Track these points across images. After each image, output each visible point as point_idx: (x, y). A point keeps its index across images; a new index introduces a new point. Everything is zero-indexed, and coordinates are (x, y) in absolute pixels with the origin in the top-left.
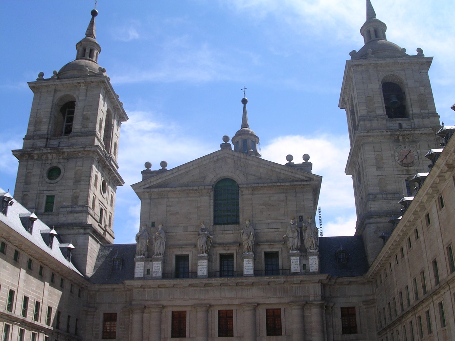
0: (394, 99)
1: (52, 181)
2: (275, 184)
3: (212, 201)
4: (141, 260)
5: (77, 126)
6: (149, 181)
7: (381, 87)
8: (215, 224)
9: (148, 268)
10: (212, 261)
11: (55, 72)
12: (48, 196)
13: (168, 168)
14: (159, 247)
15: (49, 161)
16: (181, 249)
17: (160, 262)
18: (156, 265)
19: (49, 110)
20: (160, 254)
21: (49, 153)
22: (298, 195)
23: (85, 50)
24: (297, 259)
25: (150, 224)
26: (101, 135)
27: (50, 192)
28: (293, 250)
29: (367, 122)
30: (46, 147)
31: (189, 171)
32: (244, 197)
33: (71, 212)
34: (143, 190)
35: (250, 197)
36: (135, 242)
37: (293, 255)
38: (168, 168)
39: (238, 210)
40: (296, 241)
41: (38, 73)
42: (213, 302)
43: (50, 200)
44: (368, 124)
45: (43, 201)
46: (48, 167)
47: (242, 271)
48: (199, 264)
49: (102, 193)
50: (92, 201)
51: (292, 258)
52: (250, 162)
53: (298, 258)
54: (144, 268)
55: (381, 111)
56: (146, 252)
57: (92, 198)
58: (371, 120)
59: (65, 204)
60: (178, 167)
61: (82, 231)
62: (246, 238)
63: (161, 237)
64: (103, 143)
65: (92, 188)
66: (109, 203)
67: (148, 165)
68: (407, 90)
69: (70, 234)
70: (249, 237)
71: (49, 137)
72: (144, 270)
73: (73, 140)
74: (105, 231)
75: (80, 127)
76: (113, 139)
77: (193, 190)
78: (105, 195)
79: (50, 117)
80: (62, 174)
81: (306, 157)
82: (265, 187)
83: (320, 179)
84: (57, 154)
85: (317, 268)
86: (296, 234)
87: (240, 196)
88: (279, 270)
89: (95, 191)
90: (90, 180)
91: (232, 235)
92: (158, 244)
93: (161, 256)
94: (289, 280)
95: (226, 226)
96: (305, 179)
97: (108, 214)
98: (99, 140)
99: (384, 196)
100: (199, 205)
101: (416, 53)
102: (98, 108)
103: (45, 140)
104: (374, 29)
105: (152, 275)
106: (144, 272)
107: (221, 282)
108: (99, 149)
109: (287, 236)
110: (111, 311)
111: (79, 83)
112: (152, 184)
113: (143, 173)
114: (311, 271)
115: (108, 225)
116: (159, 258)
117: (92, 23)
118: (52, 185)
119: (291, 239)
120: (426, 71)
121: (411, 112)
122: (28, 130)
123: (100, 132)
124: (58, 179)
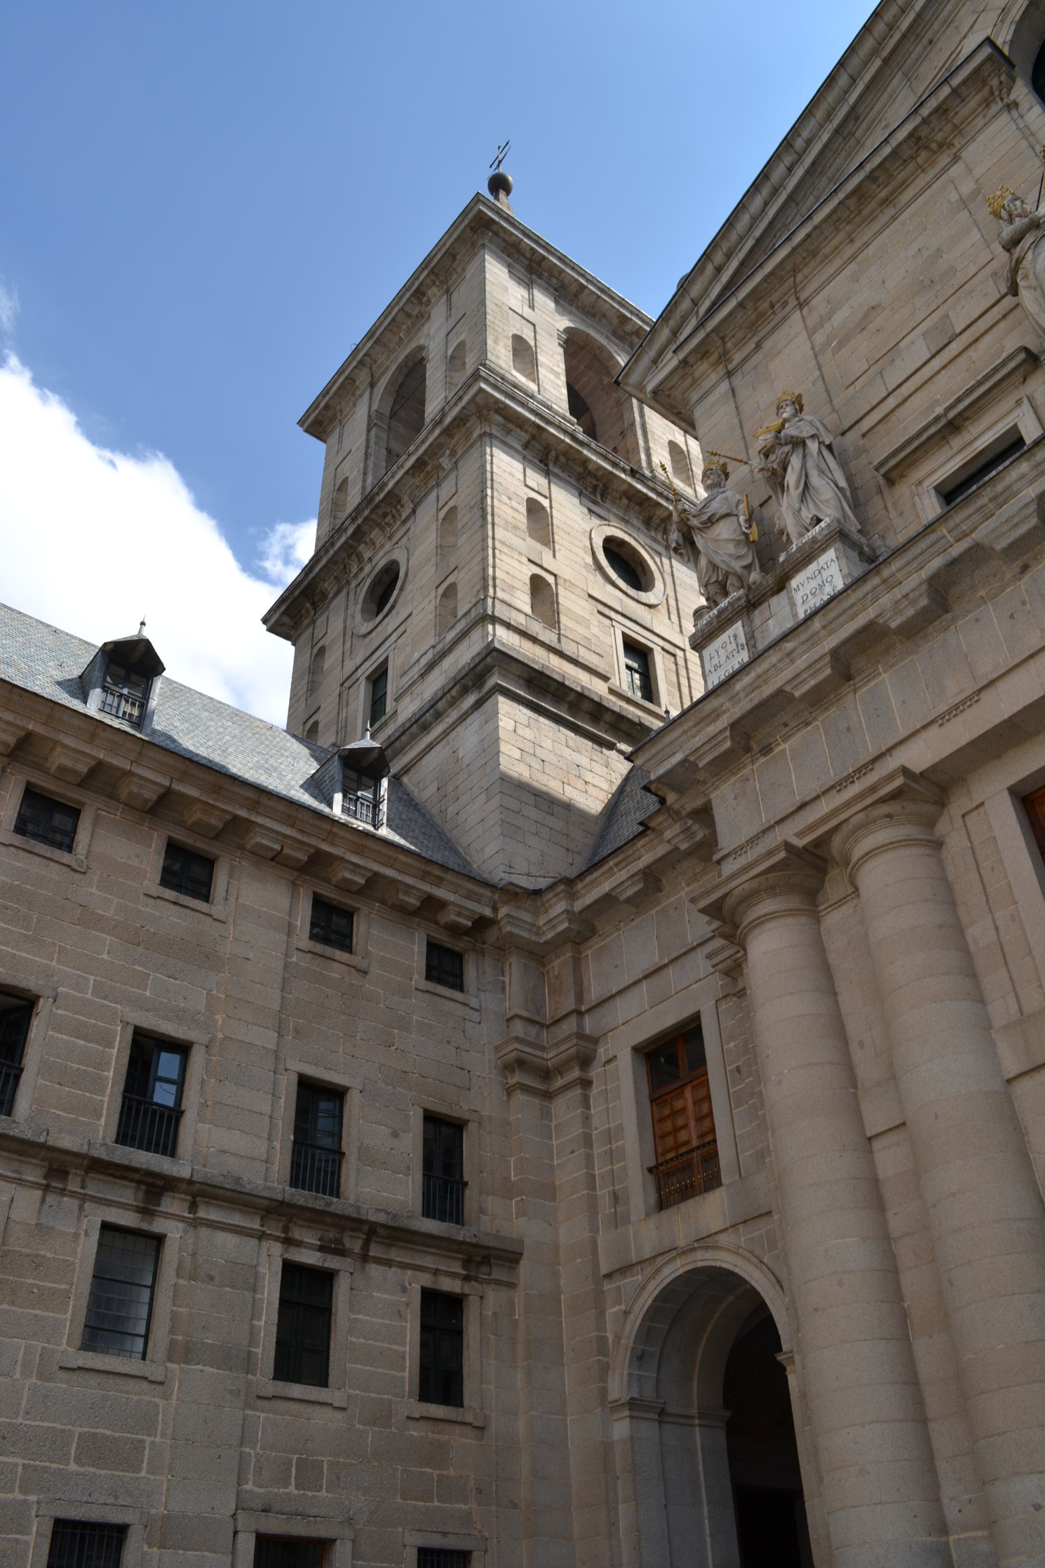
15: (367, 569)
16: (956, 442)
17: (831, 554)
18: (813, 584)
27: (375, 657)
31: (853, 116)
34: (675, 362)
60: (787, 143)
63: (799, 443)
75: (443, 395)
84: (382, 529)
100: (966, 188)
110: (669, 1017)
116: (814, 540)
118: (380, 628)
123: (535, 378)
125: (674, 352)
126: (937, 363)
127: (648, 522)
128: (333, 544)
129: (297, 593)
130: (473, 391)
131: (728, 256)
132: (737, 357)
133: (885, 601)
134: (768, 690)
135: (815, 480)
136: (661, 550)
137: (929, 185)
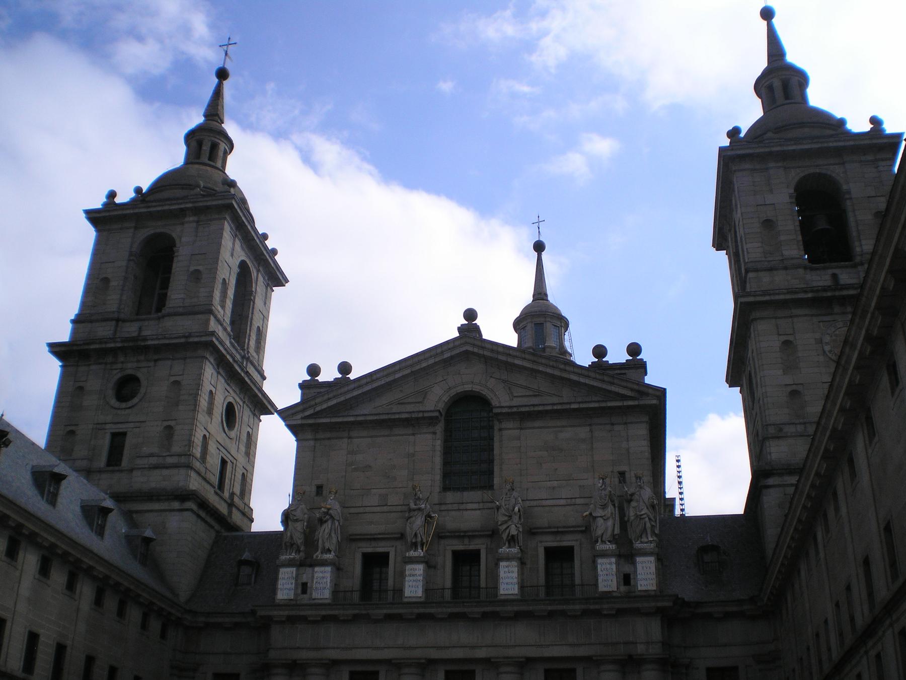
0: (822, 224)
1: (124, 405)
2: (568, 407)
3: (439, 443)
4: (290, 564)
5: (176, 295)
6: (313, 403)
7: (794, 200)
8: (445, 489)
9: (305, 580)
10: (435, 567)
11: (138, 190)
12: (114, 435)
13: (352, 376)
14: (328, 535)
15: (119, 366)
17: (329, 569)
18: (321, 575)
19: (124, 263)
20: (329, 551)
21: (119, 348)
22: (616, 428)
23: (200, 144)
24: (611, 564)
25: (314, 489)
26: (225, 312)
28: (603, 542)
29: (761, 274)
30: (113, 339)
31: (395, 381)
32: (505, 432)
33: (156, 467)
34: (299, 422)
35: (517, 432)
36: (281, 528)
37: (604, 554)
38: (352, 376)
39: (491, 462)
40: (610, 523)
41: (106, 193)
42: (435, 654)
43: (118, 439)
44: (765, 278)
45: (105, 442)
46: (116, 376)
47: (496, 588)
48: (407, 573)
49: (226, 429)
50: (200, 444)
51: (600, 561)
52: (517, 362)
53: (613, 560)
54: (296, 580)
55: (794, 251)
56: (302, 548)
57: (201, 439)
58: (771, 269)
59: (145, 450)
61: (176, 505)
62: (506, 518)
63: (332, 517)
64: (229, 329)
65: (202, 417)
66: (243, 448)
67: (314, 370)
68: (848, 203)
69: (151, 511)
70: (510, 517)
71: (122, 316)
72: (296, 584)
73: (168, 323)
74: (231, 505)
75: (182, 296)
76: (254, 322)
77: (400, 420)
78: (233, 434)
79: (126, 278)
80: (142, 390)
81: (634, 349)
82: (547, 412)
83: (661, 394)
85: (654, 582)
86: (610, 508)
87: (496, 433)
88: (573, 585)
89: (209, 424)
90: (196, 401)
91: (478, 512)
92: (327, 531)
93: (330, 556)
94: (592, 607)
95: (465, 493)
96: (629, 393)
97: (239, 472)
98: (218, 321)
99: (800, 428)
101: (867, 127)
102: (218, 259)
103: (114, 322)
104: (781, 82)
105: (311, 594)
106: (296, 588)
107: (449, 610)
108: (217, 339)
109: (591, 514)
111: (182, 210)
112: (318, 409)
113: (303, 386)
114: (640, 588)
115: (238, 493)
116: (326, 560)
117: (218, 94)
118: (123, 412)
119: (600, 521)
120: (889, 163)
121: (858, 249)
122: (84, 304)
123: (223, 307)
124: (135, 400)
125: (302, 418)
126: (378, 509)
127: (241, 390)
128: (106, 343)
129: (75, 348)
130: (208, 339)
131: (334, 397)
132: (321, 435)
133: (341, 612)
134: (302, 613)
135: (333, 535)
136: (241, 403)
137: (403, 435)
